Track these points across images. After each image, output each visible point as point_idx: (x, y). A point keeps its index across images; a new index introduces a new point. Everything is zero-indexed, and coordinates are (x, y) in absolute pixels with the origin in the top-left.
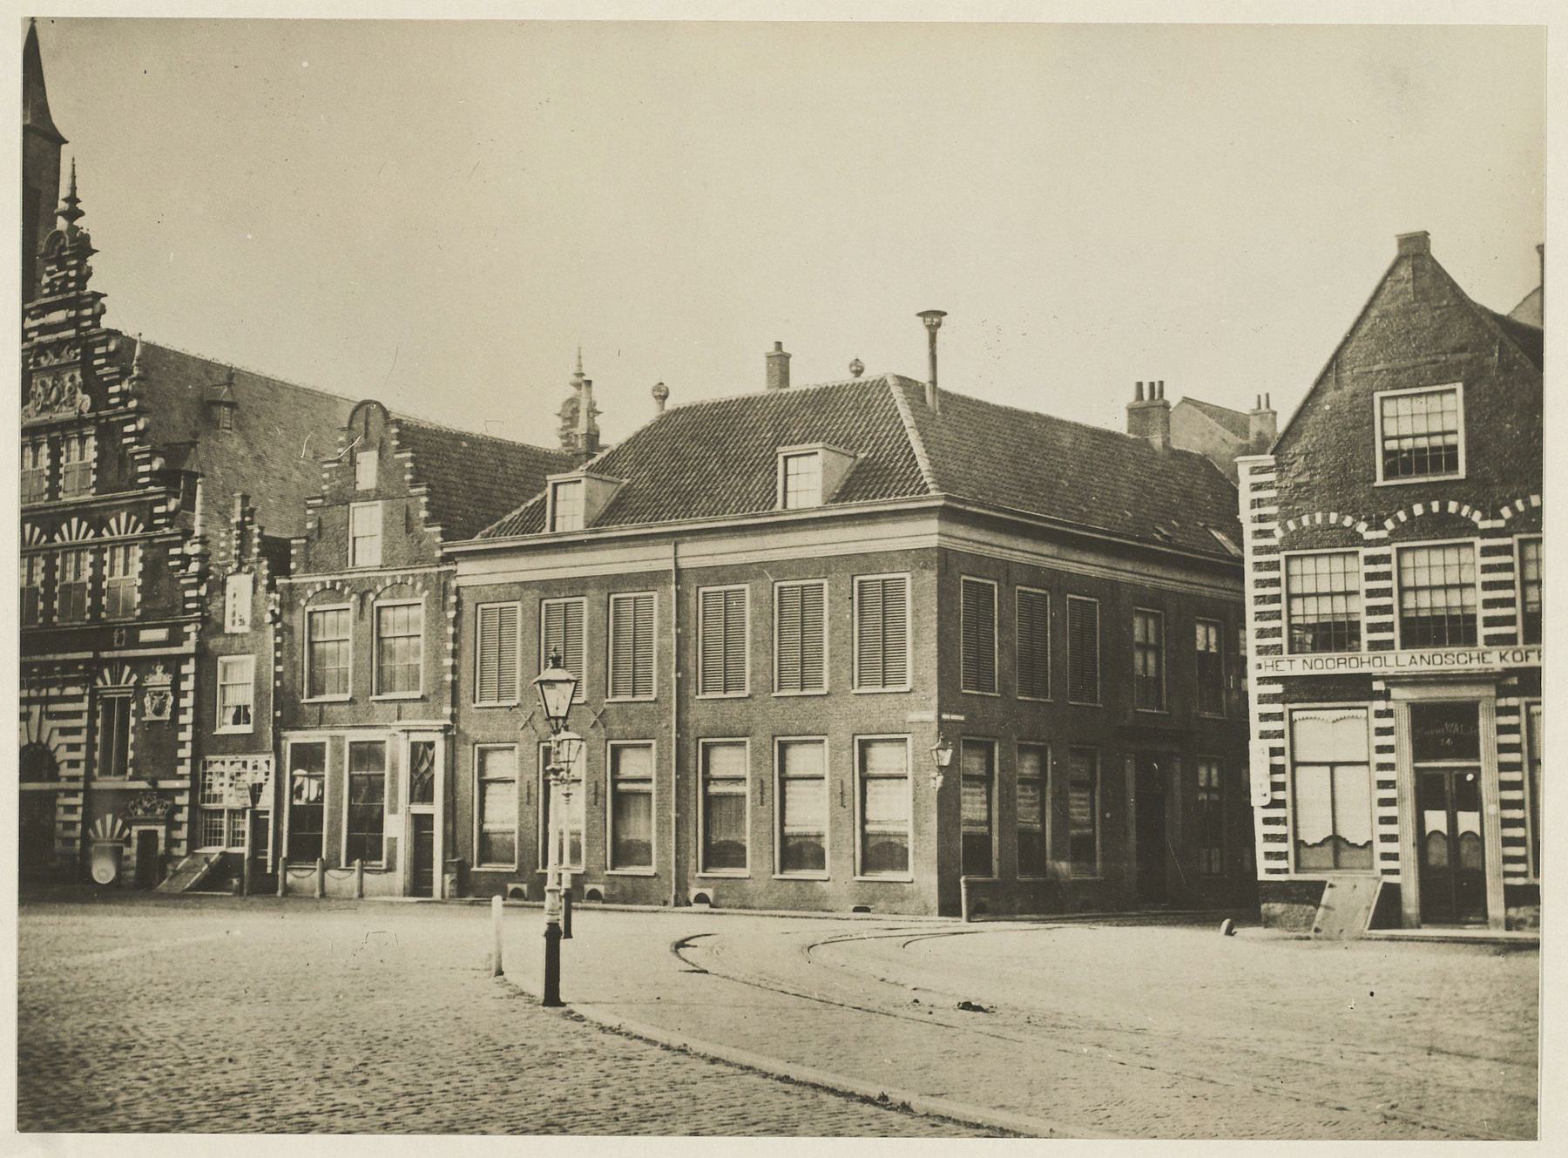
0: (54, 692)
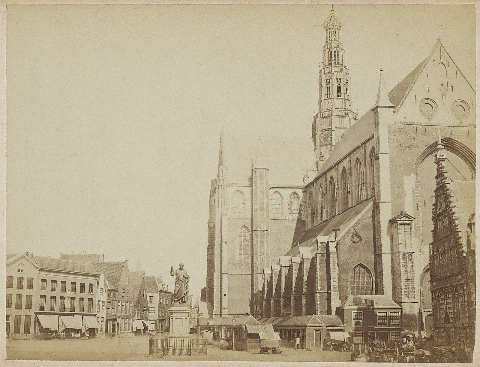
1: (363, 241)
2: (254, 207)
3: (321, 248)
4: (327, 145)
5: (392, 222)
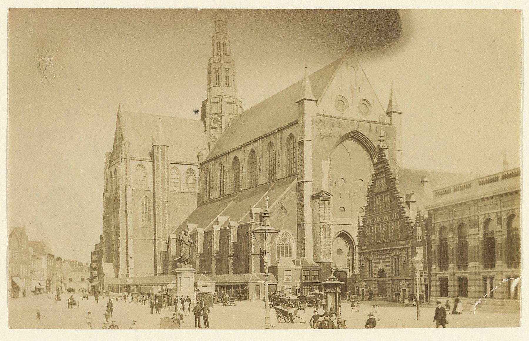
0: (384, 257)
1: (288, 213)
2: (156, 180)
3: (255, 218)
4: (217, 128)
5: (313, 198)
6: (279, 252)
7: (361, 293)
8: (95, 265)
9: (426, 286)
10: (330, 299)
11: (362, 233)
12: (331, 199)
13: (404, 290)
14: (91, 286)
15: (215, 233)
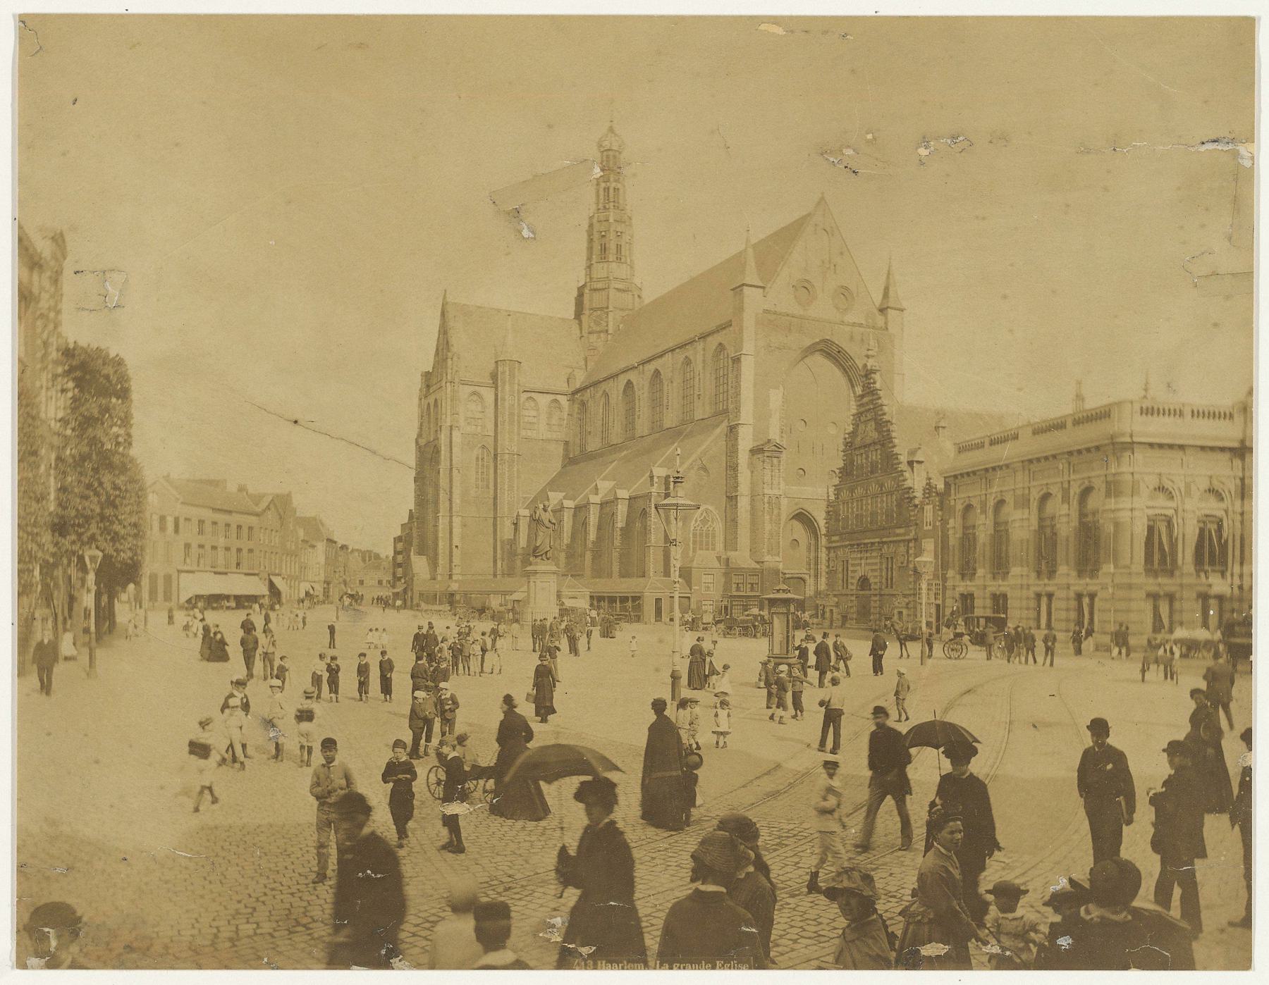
4: (600, 332)
5: (755, 451)
6: (694, 543)
7: (828, 615)
8: (400, 558)
9: (938, 606)
10: (778, 624)
11: (832, 514)
12: (784, 456)
13: (900, 613)
14: (393, 593)
15: (592, 509)
